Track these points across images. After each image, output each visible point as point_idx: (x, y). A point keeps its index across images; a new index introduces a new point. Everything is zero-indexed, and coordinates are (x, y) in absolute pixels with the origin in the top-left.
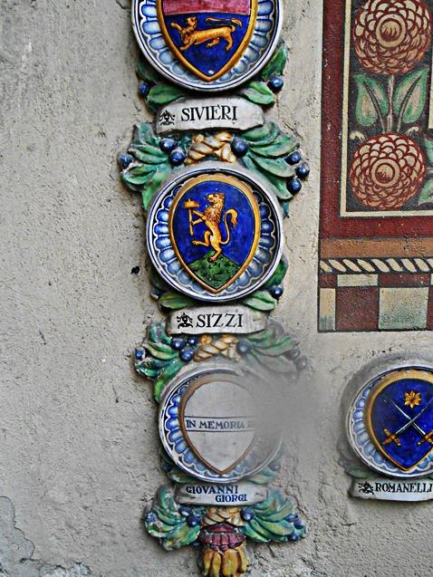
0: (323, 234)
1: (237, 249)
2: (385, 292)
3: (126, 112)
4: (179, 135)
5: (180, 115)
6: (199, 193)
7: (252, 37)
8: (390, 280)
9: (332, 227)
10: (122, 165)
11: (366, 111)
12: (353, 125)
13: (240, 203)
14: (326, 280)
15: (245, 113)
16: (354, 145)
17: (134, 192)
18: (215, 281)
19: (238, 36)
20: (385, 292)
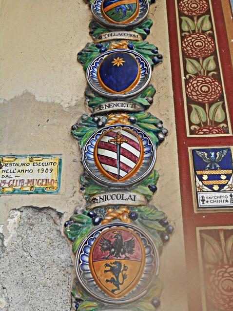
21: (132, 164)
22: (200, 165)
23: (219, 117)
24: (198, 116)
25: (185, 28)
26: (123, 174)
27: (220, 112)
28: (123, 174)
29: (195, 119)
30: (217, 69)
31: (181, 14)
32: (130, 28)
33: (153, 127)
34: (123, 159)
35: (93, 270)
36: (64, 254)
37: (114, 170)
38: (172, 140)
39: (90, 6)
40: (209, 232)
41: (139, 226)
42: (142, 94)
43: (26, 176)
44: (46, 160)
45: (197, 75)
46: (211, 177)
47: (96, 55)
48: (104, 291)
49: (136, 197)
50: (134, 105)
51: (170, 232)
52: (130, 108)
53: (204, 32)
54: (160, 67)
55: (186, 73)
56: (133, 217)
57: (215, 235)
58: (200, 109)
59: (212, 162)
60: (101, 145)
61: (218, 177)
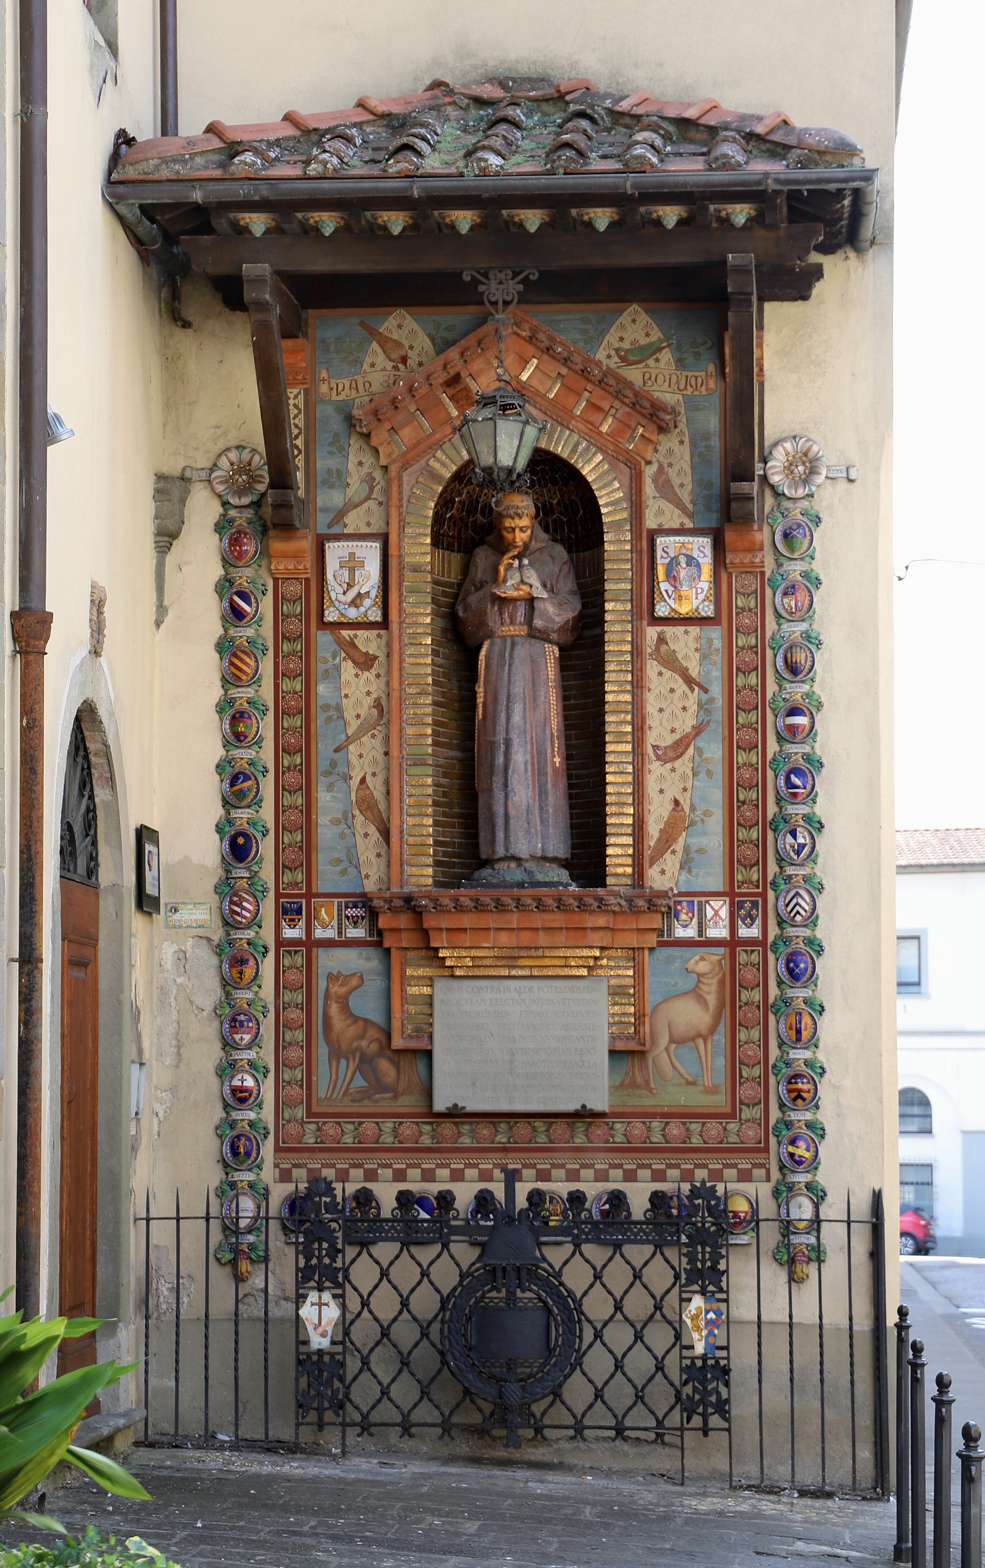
0: (275, 1151)
1: (248, 1154)
2: (294, 1170)
3: (219, 1113)
4: (234, 1121)
5: (236, 1115)
6: (238, 1137)
7: (254, 1095)
8: (296, 1166)
9: (278, 1149)
10: (217, 1128)
11: (287, 1116)
12: (283, 1119)
13: (248, 1139)
14: (276, 1166)
15: (252, 1115)
16: (283, 1125)
17: (220, 1136)
18: (242, 1163)
19: (250, 1095)
20: (294, 1170)
21: (248, 915)
22: (285, 912)
23: (299, 879)
24: (287, 877)
25: (285, 803)
26: (244, 921)
27: (300, 875)
28: (244, 921)
29: (286, 880)
30: (302, 842)
31: (284, 789)
32: (249, 807)
33: (260, 888)
34: (244, 912)
35: (230, 972)
36: (215, 961)
37: (239, 919)
38: (272, 894)
39: (222, 781)
40: (287, 951)
41: (252, 950)
42: (256, 863)
43: (193, 917)
44: (203, 907)
45: (289, 845)
46: (291, 920)
47: (227, 829)
48: (235, 982)
49: (250, 934)
50: (251, 871)
51: (267, 952)
52: (248, 875)
53: (297, 807)
54: (268, 837)
55: (283, 843)
56: (249, 944)
57: (289, 952)
58: (289, 872)
59: (292, 910)
60: (232, 902)
61: (293, 920)
